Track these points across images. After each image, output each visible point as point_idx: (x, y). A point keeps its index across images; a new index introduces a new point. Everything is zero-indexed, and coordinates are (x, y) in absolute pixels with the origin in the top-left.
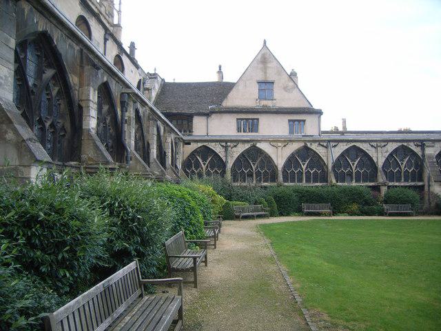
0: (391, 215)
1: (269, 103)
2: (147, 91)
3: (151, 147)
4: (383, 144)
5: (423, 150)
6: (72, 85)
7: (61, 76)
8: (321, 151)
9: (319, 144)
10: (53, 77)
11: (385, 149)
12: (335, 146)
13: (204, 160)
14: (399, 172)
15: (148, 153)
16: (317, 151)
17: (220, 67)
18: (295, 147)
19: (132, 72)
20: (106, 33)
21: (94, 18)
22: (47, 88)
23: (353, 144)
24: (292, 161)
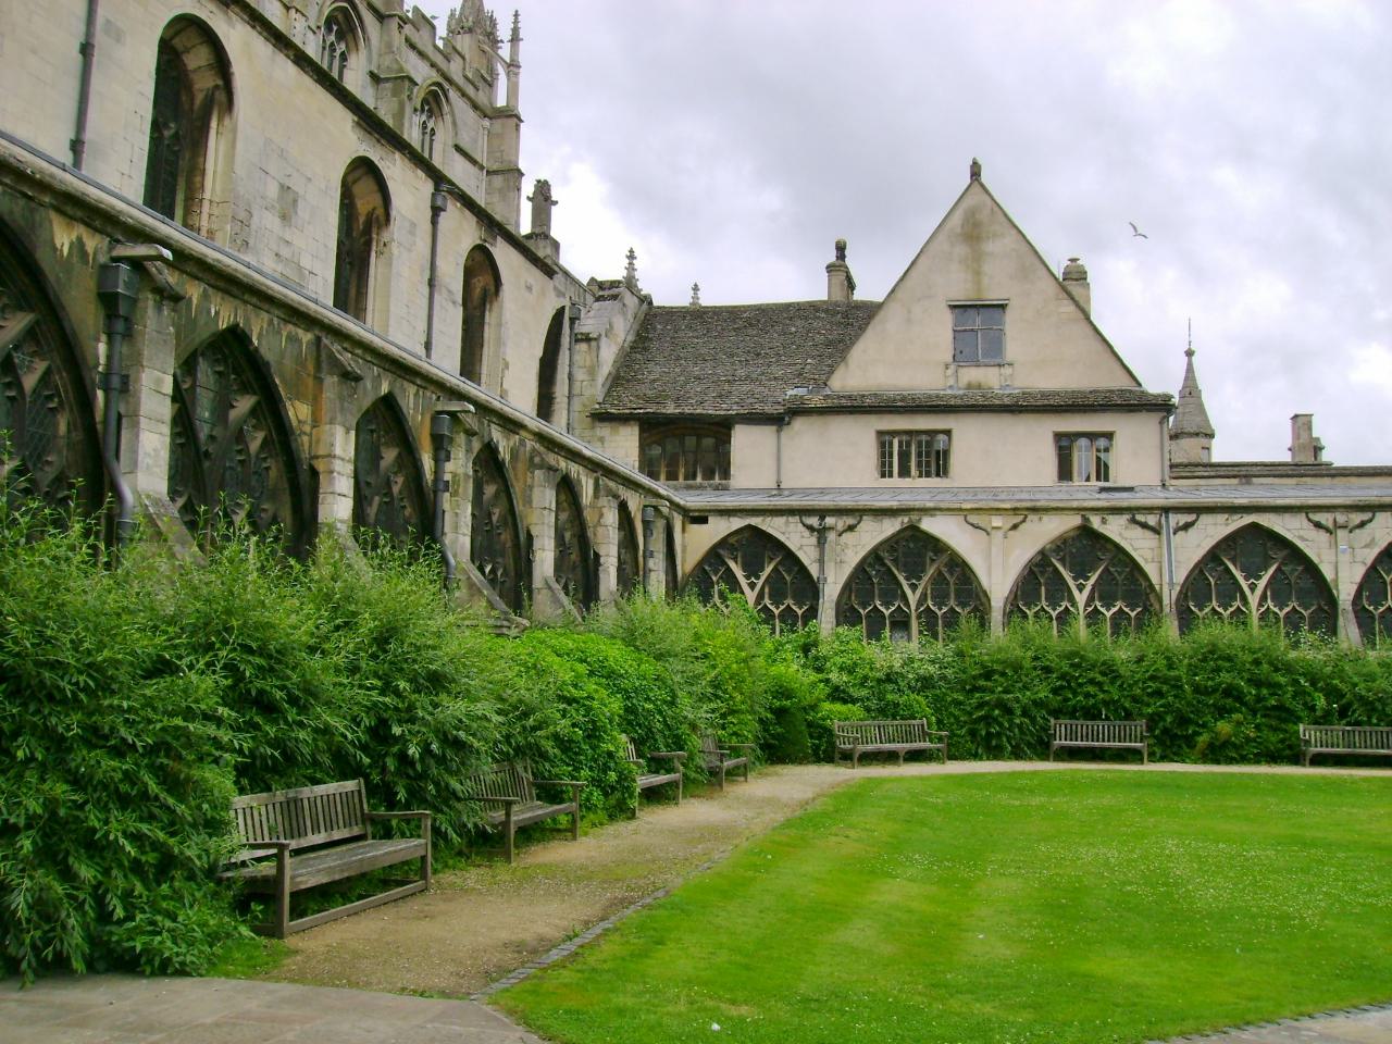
0: (1319, 760)
1: (990, 379)
2: (583, 346)
3: (537, 544)
4: (1357, 518)
6: (294, 423)
7: (271, 409)
9: (1134, 521)
10: (253, 412)
11: (1362, 535)
12: (1187, 527)
13: (752, 570)
17: (841, 249)
19: (529, 288)
20: (437, 189)
21: (398, 155)
22: (240, 437)
23: (1248, 519)
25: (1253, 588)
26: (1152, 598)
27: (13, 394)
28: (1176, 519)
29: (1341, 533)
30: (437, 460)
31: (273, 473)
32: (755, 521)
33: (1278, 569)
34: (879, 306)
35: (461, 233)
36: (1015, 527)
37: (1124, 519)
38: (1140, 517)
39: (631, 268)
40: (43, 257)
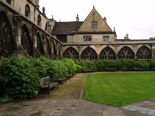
2: (50, 26)
4: (136, 45)
5: (151, 47)
8: (113, 48)
9: (113, 46)
11: (137, 47)
12: (119, 46)
13: (71, 52)
14: (143, 55)
15: (51, 51)
16: (112, 48)
17: (78, 15)
18: (104, 46)
19: (44, 20)
23: (125, 45)
24: (103, 52)
25: (126, 53)
26: (115, 54)
27: (4, 32)
28: (117, 45)
29: (135, 47)
30: (43, 40)
31: (28, 41)
32: (71, 46)
33: (128, 51)
34: (83, 22)
35: (37, 13)
36: (100, 46)
37: (112, 46)
38: (114, 45)
39: (52, 17)
40: (7, 15)
